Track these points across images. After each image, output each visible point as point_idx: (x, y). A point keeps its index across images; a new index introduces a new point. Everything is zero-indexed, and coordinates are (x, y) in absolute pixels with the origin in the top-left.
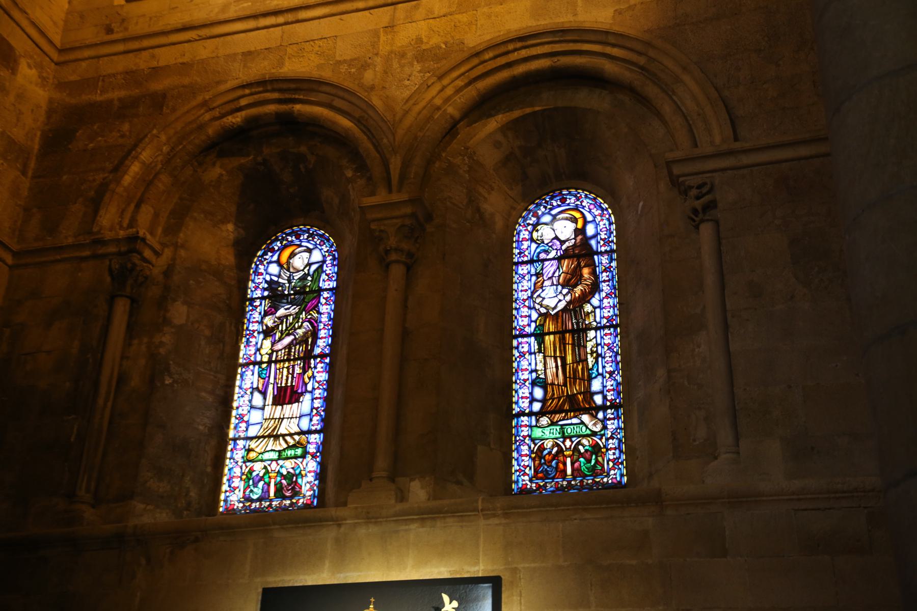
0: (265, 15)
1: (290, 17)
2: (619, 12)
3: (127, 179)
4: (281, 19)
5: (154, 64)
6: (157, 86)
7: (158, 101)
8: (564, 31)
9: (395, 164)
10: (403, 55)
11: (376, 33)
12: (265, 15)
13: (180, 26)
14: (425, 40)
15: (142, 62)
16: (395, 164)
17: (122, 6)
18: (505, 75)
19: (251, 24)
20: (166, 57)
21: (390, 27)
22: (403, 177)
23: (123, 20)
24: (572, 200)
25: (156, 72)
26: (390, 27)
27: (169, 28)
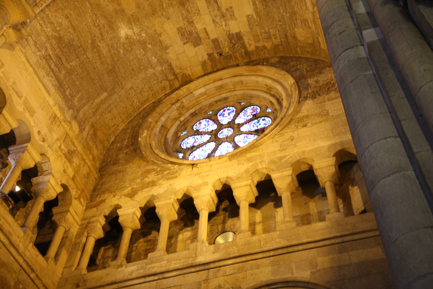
0: (149, 276)
1: (161, 276)
2: (313, 273)
4: (156, 278)
8: (288, 282)
12: (149, 276)
13: (110, 282)
14: (223, 286)
17: (85, 274)
19: (143, 280)
23: (85, 281)
27: (105, 283)
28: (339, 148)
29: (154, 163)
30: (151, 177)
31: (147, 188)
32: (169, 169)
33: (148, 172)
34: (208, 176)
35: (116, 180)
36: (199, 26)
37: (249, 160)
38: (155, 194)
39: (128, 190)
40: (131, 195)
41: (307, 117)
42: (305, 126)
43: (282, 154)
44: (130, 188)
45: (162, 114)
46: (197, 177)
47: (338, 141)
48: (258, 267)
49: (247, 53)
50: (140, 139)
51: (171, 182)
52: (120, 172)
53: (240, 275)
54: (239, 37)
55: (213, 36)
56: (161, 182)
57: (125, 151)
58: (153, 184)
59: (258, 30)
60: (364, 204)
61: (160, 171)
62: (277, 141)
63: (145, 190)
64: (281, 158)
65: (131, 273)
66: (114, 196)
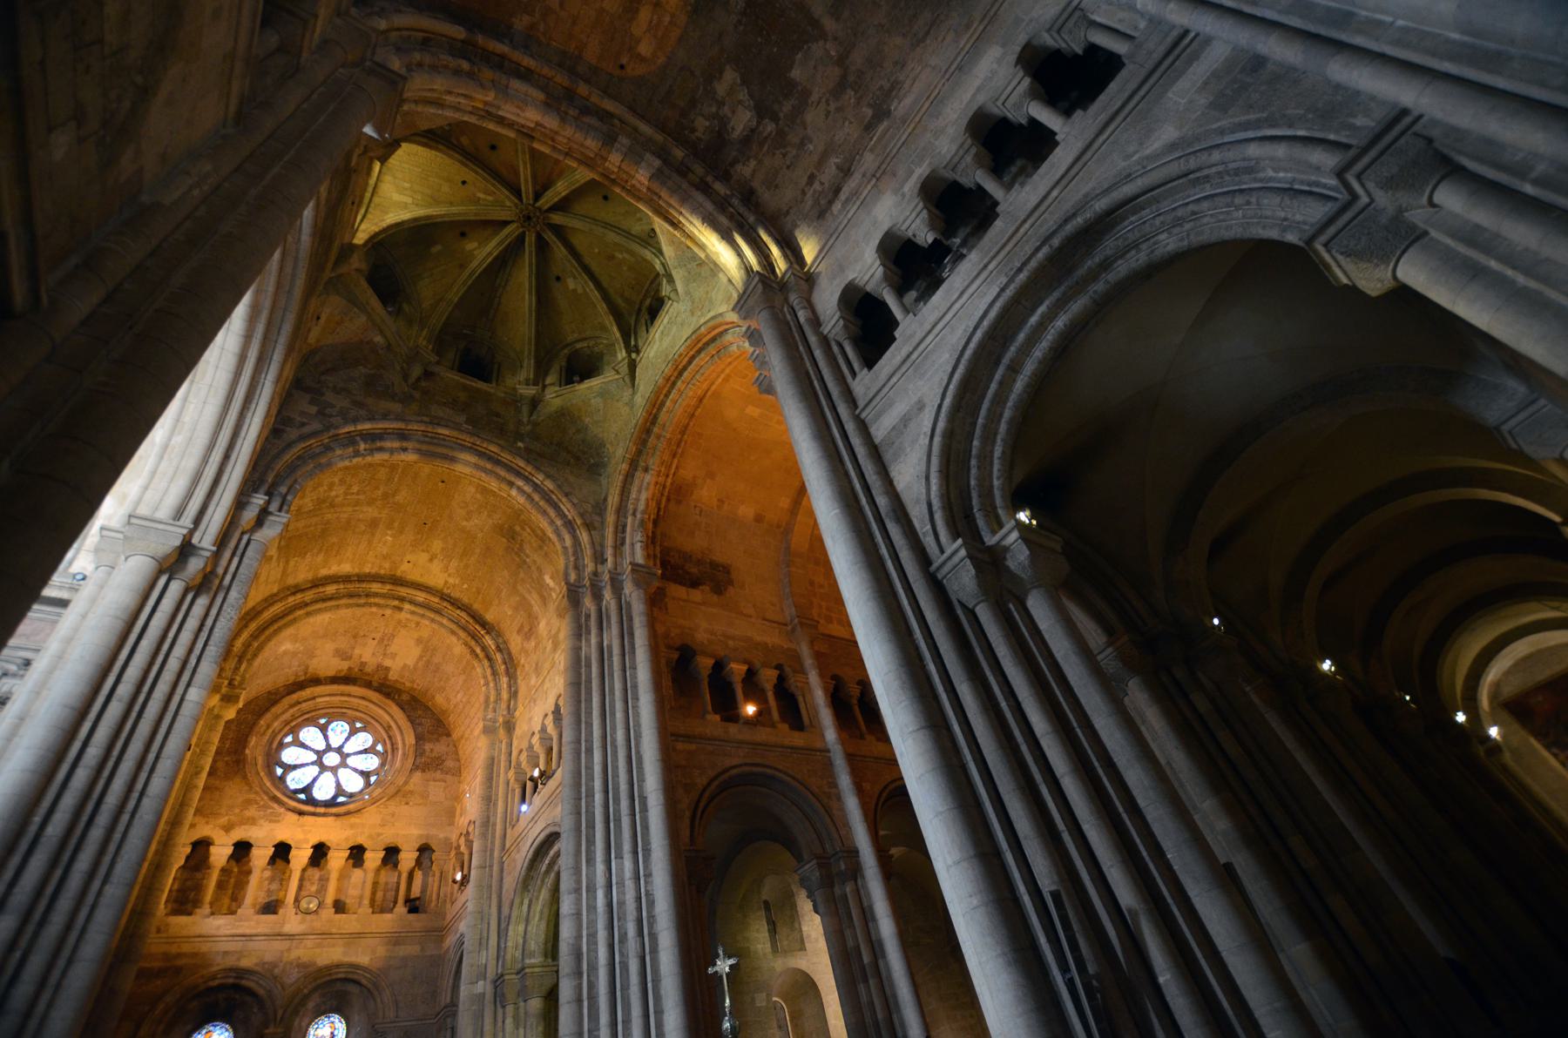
2: (371, 959)
3: (157, 1012)
4: (244, 939)
5: (179, 951)
6: (179, 962)
7: (178, 970)
9: (280, 1013)
10: (291, 964)
11: (282, 952)
15: (174, 950)
16: (280, 1013)
18: (328, 978)
19: (231, 938)
20: (186, 948)
21: (289, 950)
22: (282, 1018)
24: (332, 1019)
25: (179, 955)
26: (289, 950)
28: (424, 841)
29: (256, 793)
30: (252, 812)
31: (244, 824)
32: (273, 808)
33: (248, 802)
34: (310, 831)
35: (211, 800)
36: (357, 651)
37: (352, 826)
38: (254, 836)
39: (223, 820)
40: (228, 829)
41: (411, 792)
42: (407, 804)
43: (380, 830)
44: (226, 818)
45: (277, 717)
46: (299, 829)
47: (426, 833)
48: (334, 946)
49: (387, 675)
50: (247, 751)
51: (273, 825)
52: (217, 789)
53: (318, 951)
54: (387, 669)
55: (363, 660)
56: (262, 821)
57: (226, 759)
58: (252, 821)
59: (407, 674)
60: (421, 892)
61: (263, 806)
62: (381, 813)
63: (243, 827)
64: (379, 835)
65: (218, 928)
66: (207, 823)
